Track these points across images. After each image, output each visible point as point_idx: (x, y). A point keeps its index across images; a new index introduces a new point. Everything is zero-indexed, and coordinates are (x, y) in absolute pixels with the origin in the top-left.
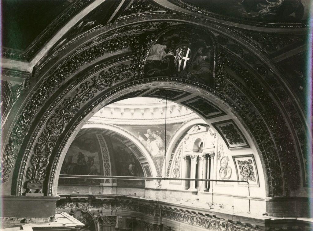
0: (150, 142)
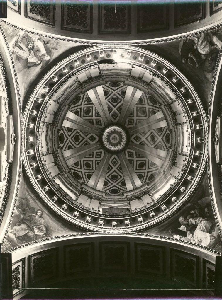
0: (193, 235)
